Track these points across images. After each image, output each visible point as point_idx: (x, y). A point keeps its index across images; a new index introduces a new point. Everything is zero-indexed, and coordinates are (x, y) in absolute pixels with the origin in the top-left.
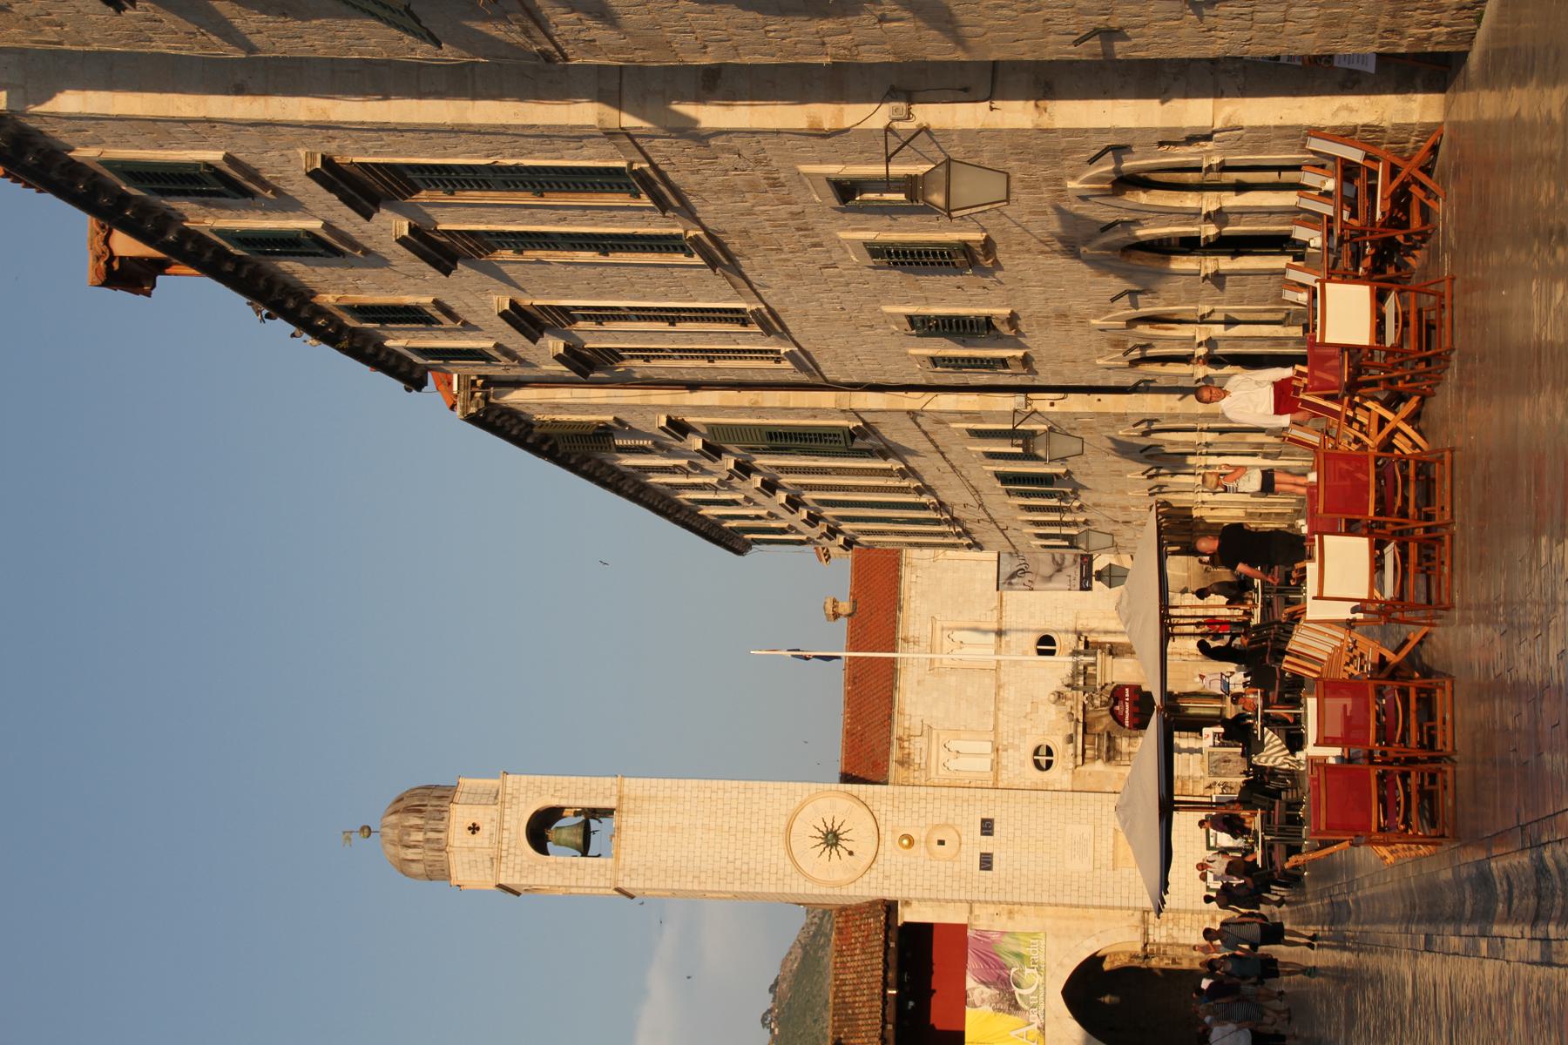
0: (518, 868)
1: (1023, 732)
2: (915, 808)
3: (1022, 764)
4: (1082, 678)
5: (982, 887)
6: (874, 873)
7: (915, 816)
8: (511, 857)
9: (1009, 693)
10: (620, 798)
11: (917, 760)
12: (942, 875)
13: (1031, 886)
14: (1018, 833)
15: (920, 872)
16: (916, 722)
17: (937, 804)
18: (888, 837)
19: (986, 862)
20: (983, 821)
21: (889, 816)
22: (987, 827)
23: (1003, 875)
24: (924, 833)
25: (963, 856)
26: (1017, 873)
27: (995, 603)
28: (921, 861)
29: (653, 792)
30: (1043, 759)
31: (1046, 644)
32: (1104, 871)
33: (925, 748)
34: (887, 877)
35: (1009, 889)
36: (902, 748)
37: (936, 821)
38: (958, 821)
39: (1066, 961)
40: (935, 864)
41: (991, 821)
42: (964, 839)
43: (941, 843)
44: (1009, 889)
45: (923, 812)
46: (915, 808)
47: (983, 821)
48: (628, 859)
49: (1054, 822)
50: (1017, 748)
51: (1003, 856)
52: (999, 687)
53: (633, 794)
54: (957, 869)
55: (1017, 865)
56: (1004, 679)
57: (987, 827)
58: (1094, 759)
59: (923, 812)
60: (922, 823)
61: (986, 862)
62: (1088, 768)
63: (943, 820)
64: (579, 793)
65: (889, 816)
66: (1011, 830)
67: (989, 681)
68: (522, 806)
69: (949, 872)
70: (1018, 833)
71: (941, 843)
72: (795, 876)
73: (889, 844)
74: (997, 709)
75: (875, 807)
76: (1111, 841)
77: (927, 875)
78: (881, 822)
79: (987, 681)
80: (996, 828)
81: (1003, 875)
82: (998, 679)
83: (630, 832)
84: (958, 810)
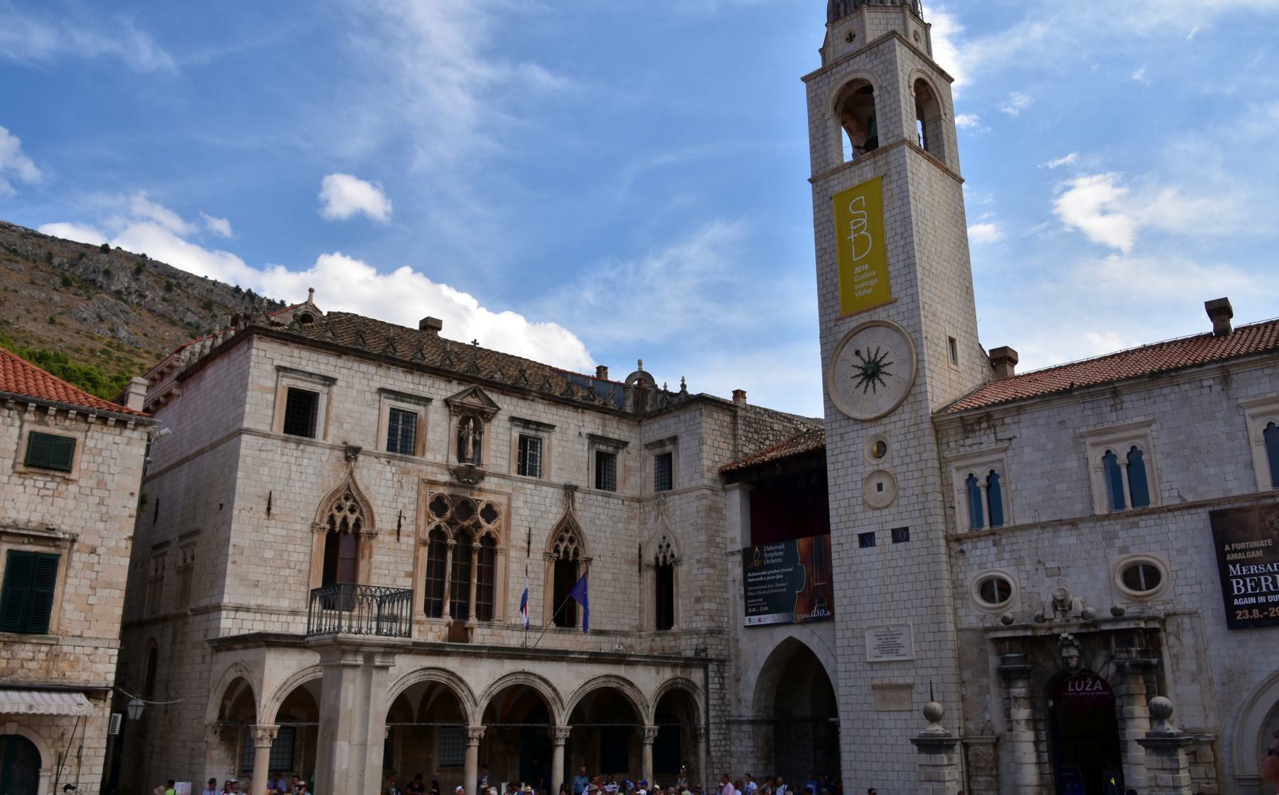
0: (819, 91)
1: (1018, 562)
2: (910, 451)
3: (981, 566)
4: (1093, 635)
5: (842, 540)
6: (844, 423)
7: (902, 453)
8: (826, 81)
9: (1067, 538)
10: (886, 149)
11: (968, 442)
12: (848, 495)
13: (850, 593)
14: (898, 571)
15: (851, 470)
16: (1013, 430)
17: (917, 474)
18: (877, 430)
19: (866, 540)
20: (906, 529)
21: (900, 424)
22: (900, 535)
23: (856, 560)
24: (886, 467)
25: (869, 514)
26: (859, 576)
27: (1190, 499)
28: (860, 469)
29: (895, 177)
30: (995, 590)
31: (1142, 576)
32: (870, 674)
33: (984, 447)
34: (842, 439)
35: (845, 569)
36: (979, 421)
37: (900, 477)
38: (903, 501)
39: (816, 639)
40: (859, 485)
41: (907, 539)
42: (886, 512)
43: (880, 487)
44: (845, 569)
45: (907, 460)
46: (910, 451)
47: (906, 529)
48: (835, 182)
49: (913, 612)
50: (999, 558)
51: (873, 558)
52: (1073, 523)
53: (891, 159)
54: (857, 509)
55: (866, 575)
56: (1085, 528)
57: (900, 535)
58: (1000, 653)
59: (907, 460)
60: (896, 462)
61: (866, 540)
62: (990, 648)
63: (902, 484)
64: (887, 109)
65: (900, 424)
66: (900, 563)
67: (1078, 509)
68: (870, 65)
69: (853, 502)
70: (898, 571)
71: (880, 487)
72: (835, 344)
73: (872, 431)
74: (1043, 526)
75: (907, 408)
76: (901, 681)
77: (849, 479)
78: (894, 418)
79: (1079, 507)
80: (901, 545)
81: (856, 560)
82: (1082, 520)
83: (857, 173)
84: (913, 499)
